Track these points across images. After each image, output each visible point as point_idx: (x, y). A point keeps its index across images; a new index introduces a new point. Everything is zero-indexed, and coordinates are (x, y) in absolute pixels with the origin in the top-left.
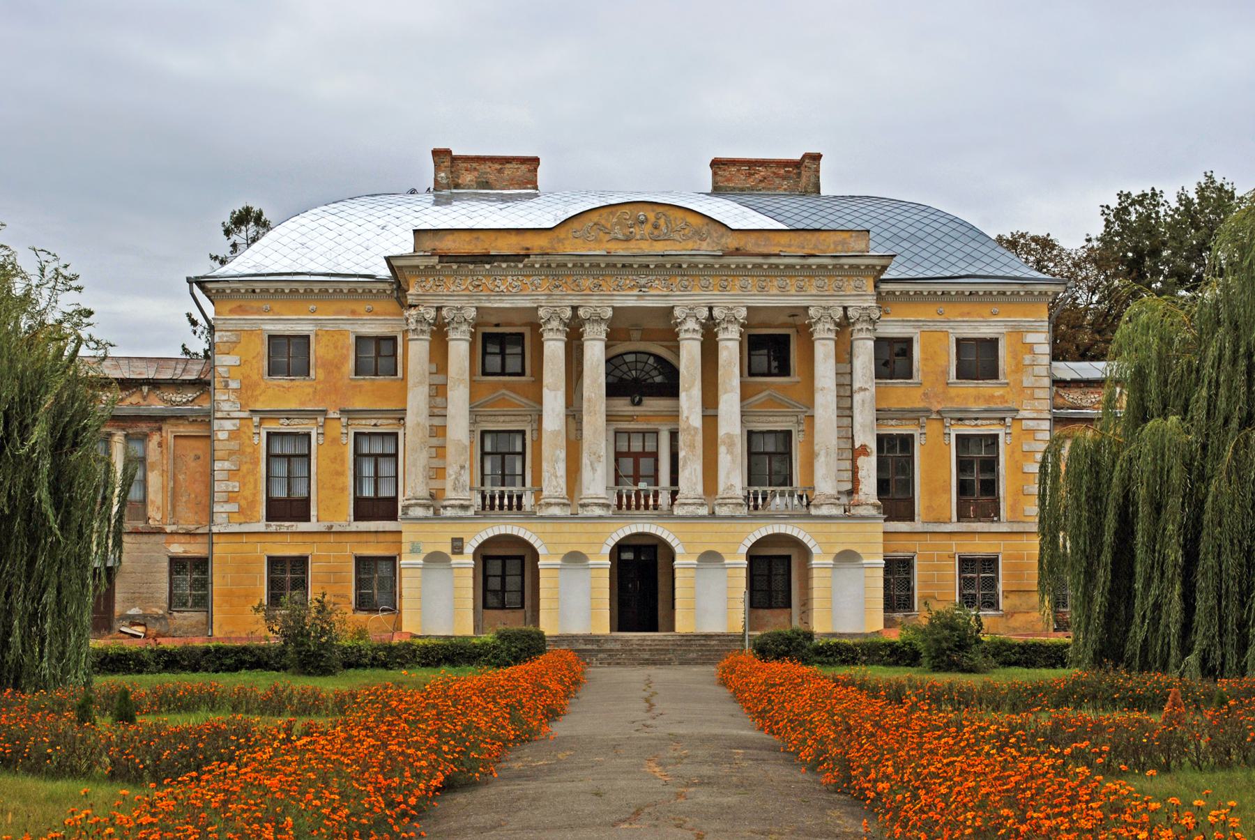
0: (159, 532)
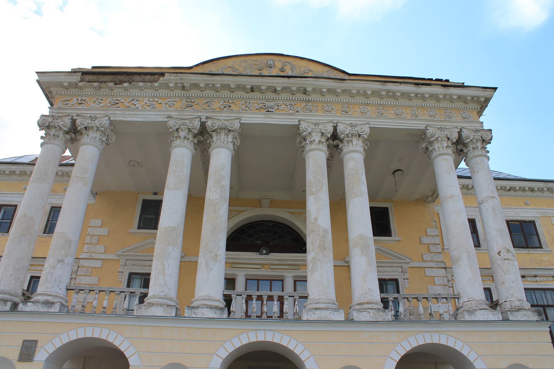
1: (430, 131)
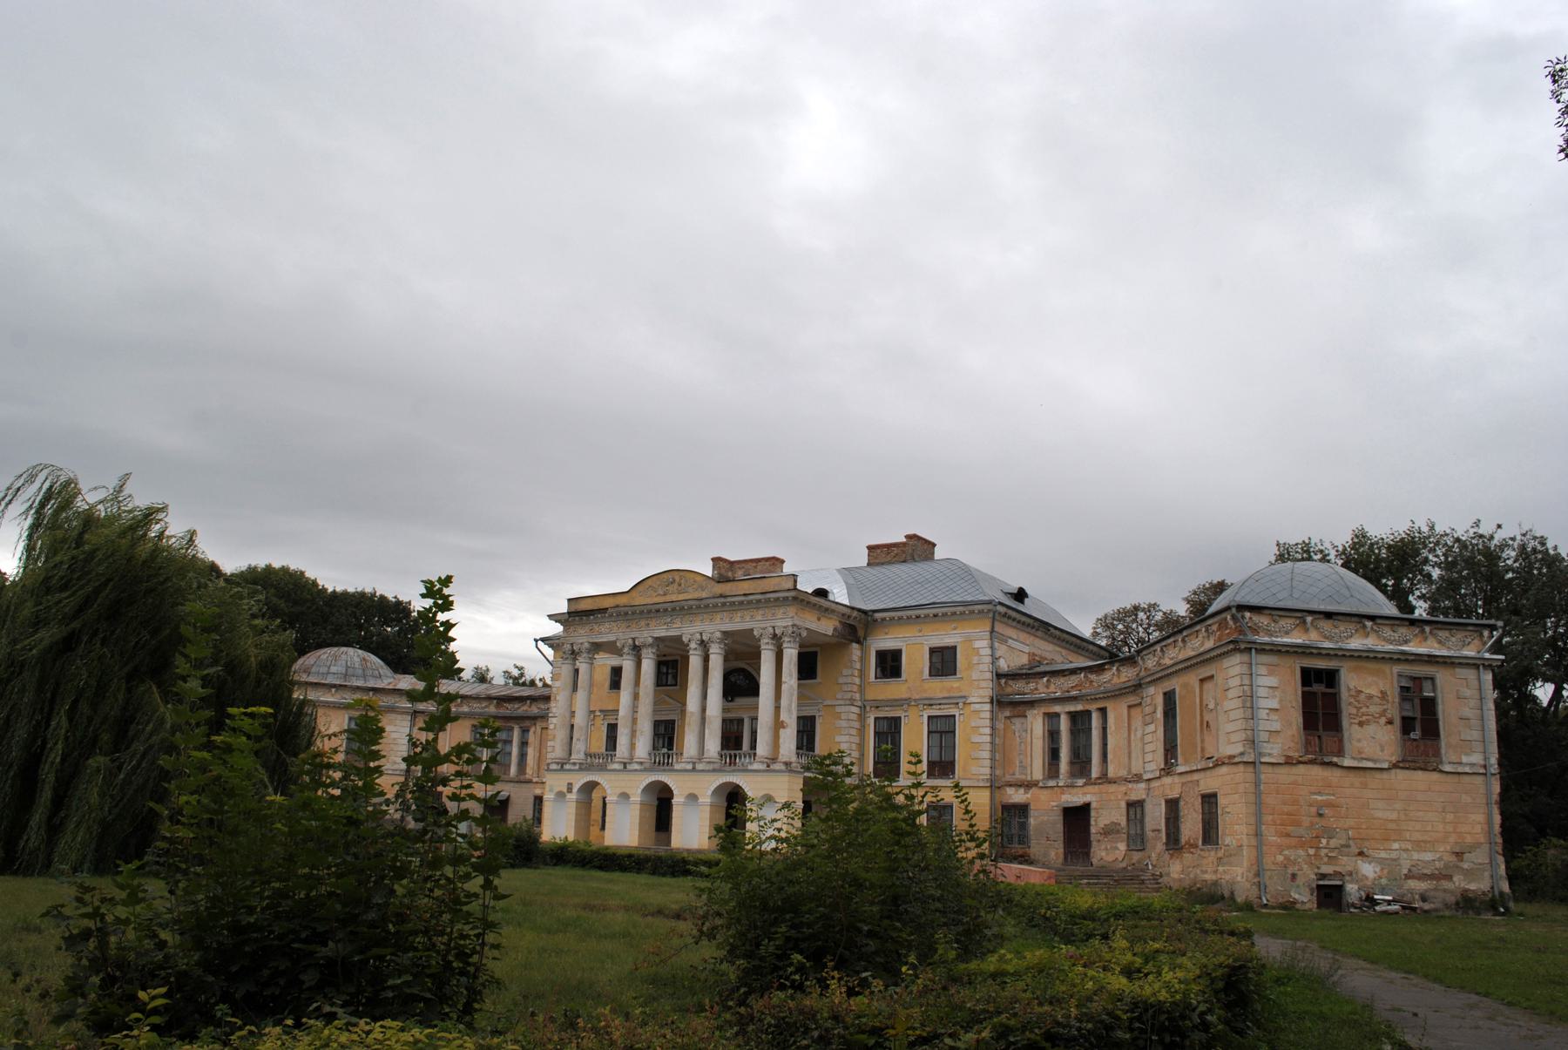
0: (530, 781)
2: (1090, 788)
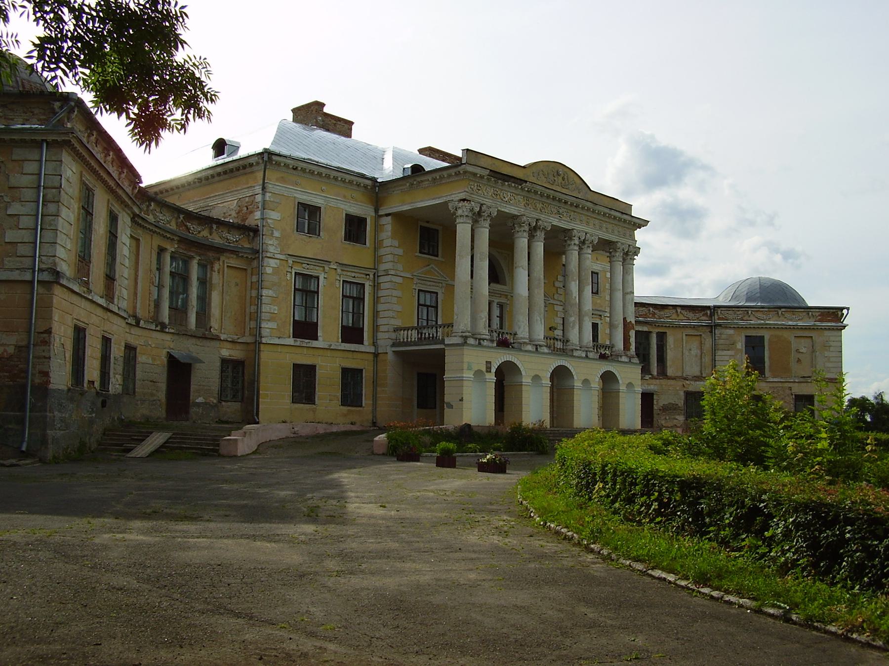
0: (217, 338)
1: (619, 245)
2: (654, 381)
